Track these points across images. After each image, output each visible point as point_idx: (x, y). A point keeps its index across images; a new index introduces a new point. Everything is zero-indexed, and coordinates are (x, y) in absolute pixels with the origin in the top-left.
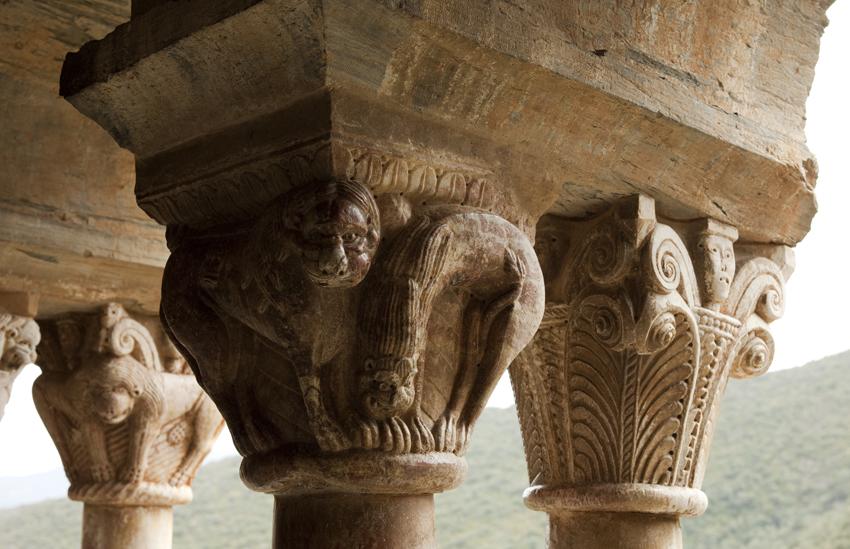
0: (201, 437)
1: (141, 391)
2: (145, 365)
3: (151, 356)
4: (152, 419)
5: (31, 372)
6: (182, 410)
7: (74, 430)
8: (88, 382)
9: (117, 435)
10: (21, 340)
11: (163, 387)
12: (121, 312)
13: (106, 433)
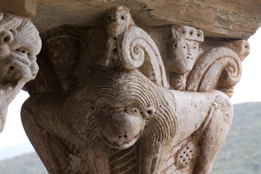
0: (208, 159)
1: (153, 108)
2: (154, 81)
3: (159, 70)
4: (164, 142)
5: (23, 96)
6: (192, 130)
7: (71, 156)
8: (93, 102)
9: (122, 161)
10: (18, 46)
11: (175, 104)
12: (129, 19)
13: (111, 159)
